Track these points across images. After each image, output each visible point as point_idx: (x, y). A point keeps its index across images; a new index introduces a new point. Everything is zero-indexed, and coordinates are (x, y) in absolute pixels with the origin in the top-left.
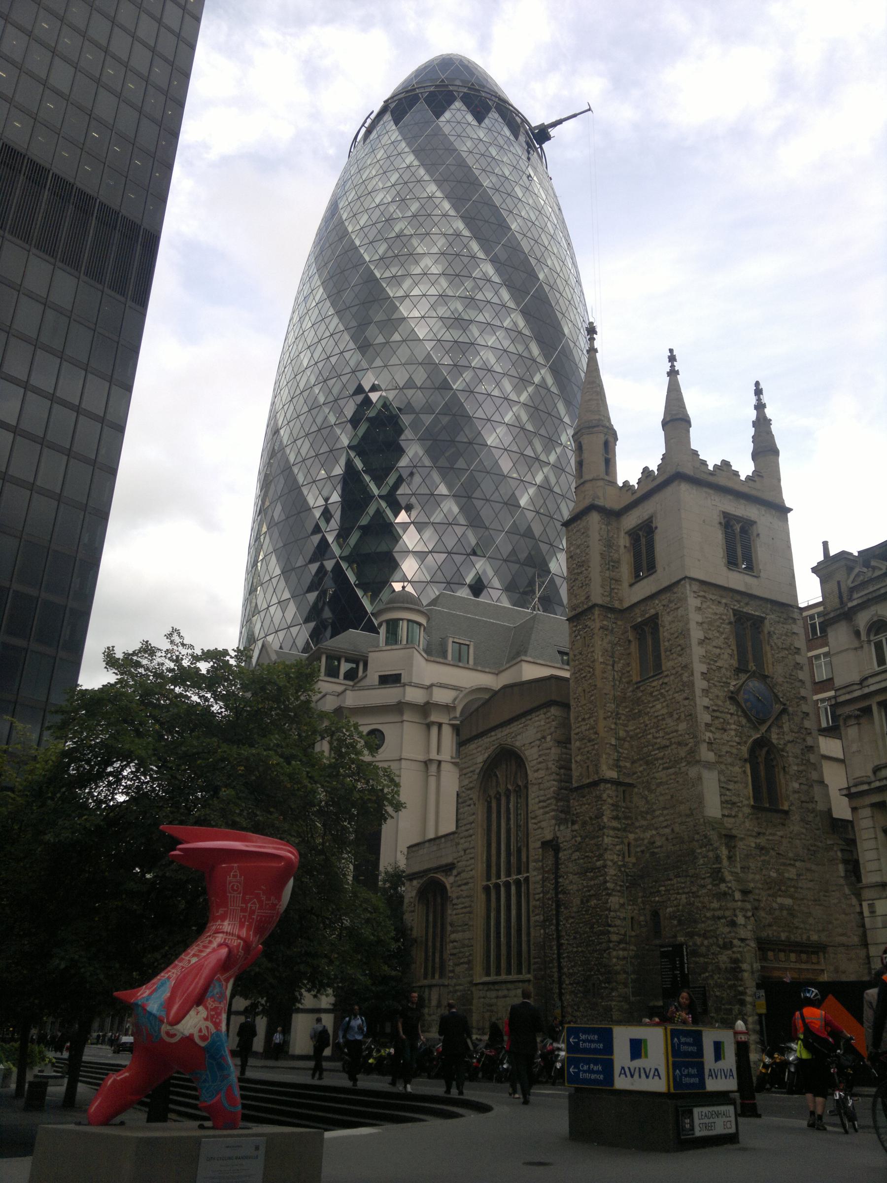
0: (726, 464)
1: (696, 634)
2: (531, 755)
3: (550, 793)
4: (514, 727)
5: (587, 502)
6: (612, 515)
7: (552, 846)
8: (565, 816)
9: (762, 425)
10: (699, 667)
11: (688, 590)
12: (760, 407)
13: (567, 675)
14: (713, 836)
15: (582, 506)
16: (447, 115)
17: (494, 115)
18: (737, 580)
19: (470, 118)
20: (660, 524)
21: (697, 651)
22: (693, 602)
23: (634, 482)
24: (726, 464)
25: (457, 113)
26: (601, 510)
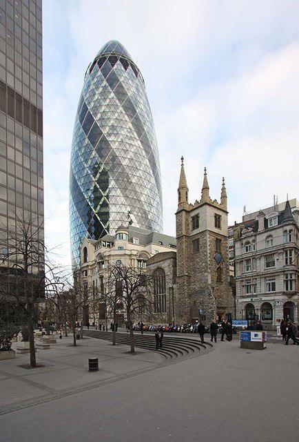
0: (216, 200)
1: (208, 243)
2: (166, 270)
3: (171, 278)
4: (161, 263)
5: (182, 208)
6: (188, 212)
7: (172, 288)
8: (174, 283)
9: (223, 189)
10: (208, 251)
11: (207, 233)
12: (223, 184)
13: (176, 251)
14: (210, 287)
15: (180, 210)
16: (116, 66)
17: (130, 67)
18: (216, 230)
19: (123, 68)
20: (201, 216)
21: (209, 247)
22: (208, 236)
23: (193, 204)
24: (216, 200)
25: (118, 66)
26: (185, 211)
